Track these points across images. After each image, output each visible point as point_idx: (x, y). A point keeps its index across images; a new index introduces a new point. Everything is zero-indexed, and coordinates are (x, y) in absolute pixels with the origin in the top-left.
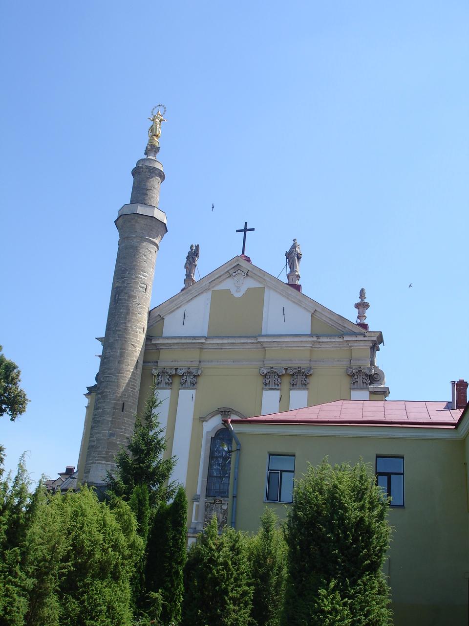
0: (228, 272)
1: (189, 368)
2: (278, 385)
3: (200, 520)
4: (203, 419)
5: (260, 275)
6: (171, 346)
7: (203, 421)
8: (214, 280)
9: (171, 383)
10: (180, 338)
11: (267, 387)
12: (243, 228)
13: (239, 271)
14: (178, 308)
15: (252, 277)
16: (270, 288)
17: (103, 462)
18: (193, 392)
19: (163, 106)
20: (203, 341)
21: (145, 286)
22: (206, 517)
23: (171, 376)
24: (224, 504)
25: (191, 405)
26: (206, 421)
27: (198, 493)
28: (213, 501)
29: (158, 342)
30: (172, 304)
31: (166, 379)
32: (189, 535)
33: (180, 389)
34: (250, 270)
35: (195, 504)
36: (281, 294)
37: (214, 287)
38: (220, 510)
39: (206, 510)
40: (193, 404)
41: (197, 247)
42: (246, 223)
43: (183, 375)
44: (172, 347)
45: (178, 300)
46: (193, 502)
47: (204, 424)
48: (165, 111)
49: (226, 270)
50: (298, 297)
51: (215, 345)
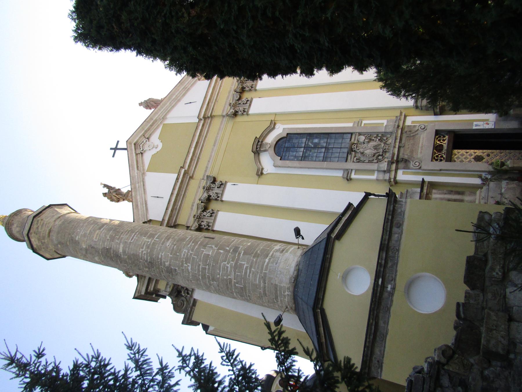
0: (137, 154)
1: (204, 188)
2: (248, 101)
3: (375, 166)
4: (260, 173)
5: (151, 123)
6: (176, 209)
7: (262, 173)
8: (138, 167)
9: (212, 210)
10: (172, 194)
11: (246, 110)
12: (113, 151)
13: (141, 145)
14: (146, 204)
15: (151, 135)
16: (164, 118)
17: (267, 260)
18: (229, 185)
20: (183, 171)
22: (370, 162)
23: (205, 209)
24: (358, 141)
25: (241, 186)
26: (262, 169)
27: (340, 174)
28: (354, 153)
29: (166, 222)
30: (139, 208)
31: (207, 214)
32: (392, 177)
33: (222, 201)
34: (143, 132)
35: (353, 176)
36: (173, 107)
37: (144, 170)
38: (365, 145)
39: (364, 162)
40: (240, 185)
41: (105, 186)
42: (111, 149)
43: (210, 196)
44: (178, 208)
45: (139, 200)
46: (351, 179)
47: (264, 173)
49: (134, 154)
50: (180, 90)
51: (192, 163)
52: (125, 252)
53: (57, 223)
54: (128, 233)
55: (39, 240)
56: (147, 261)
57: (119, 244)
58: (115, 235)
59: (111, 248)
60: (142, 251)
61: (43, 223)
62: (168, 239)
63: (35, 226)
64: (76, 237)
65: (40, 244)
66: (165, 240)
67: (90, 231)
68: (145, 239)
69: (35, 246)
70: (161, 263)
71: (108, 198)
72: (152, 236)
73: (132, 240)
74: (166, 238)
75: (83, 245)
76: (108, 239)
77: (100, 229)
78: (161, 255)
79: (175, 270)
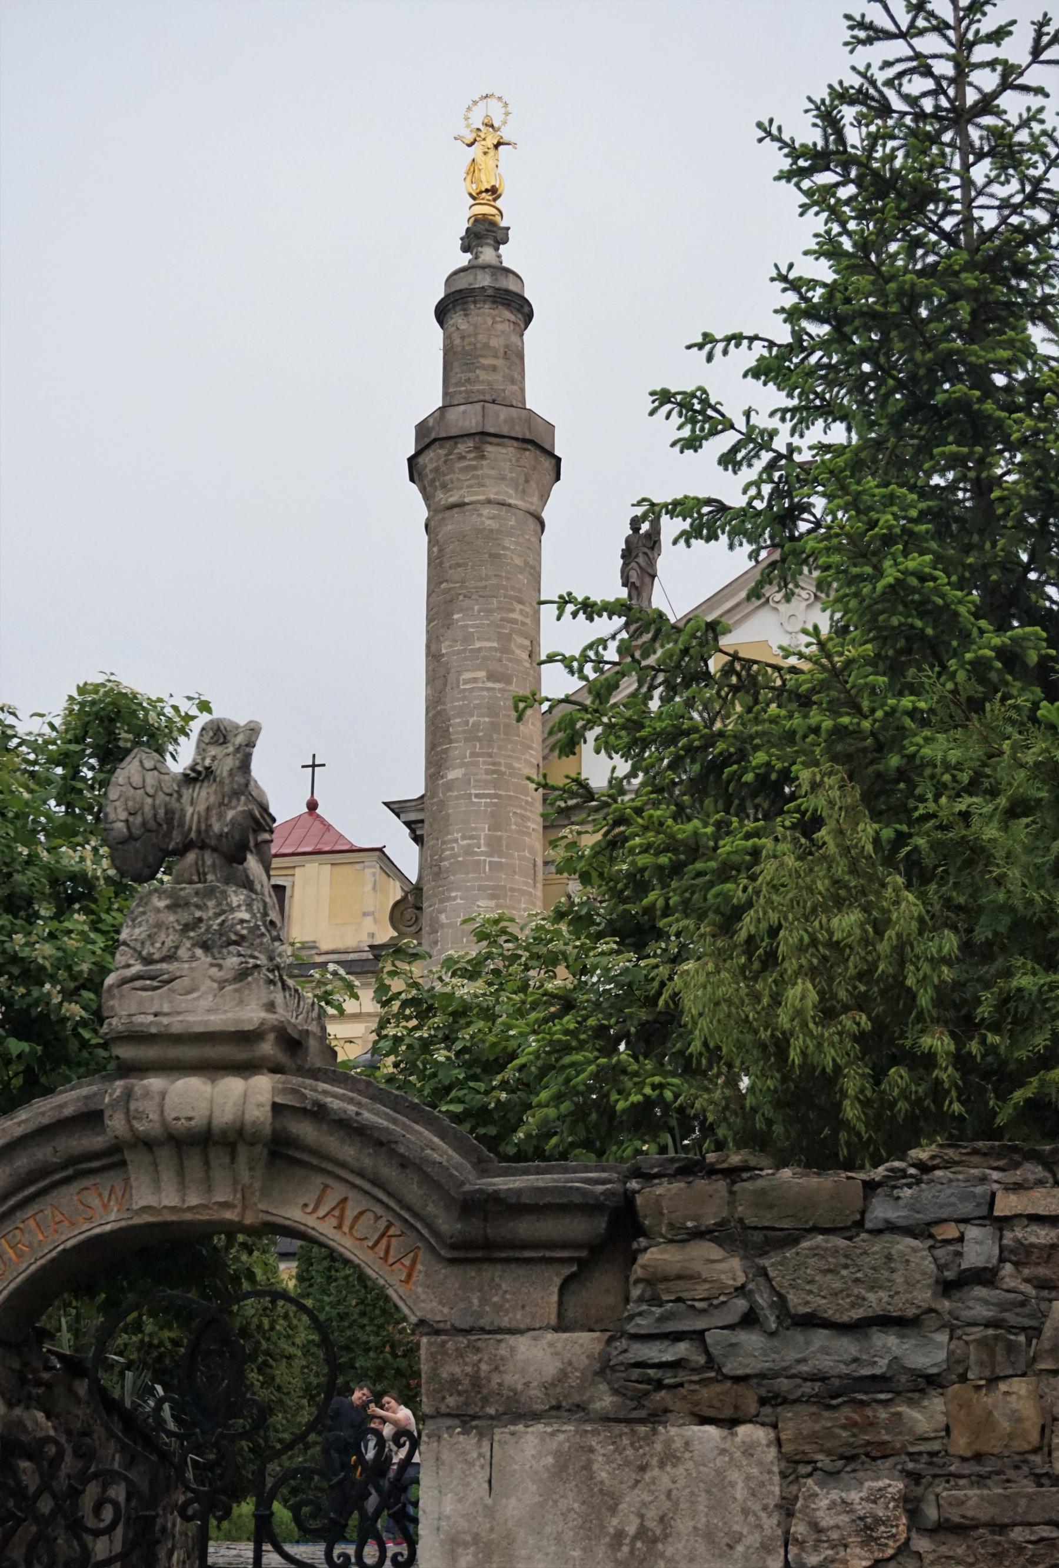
19: (500, 98)
21: (527, 643)
48: (507, 114)
52: (449, 790)
53: (486, 511)
54: (494, 772)
55: (436, 470)
56: (442, 860)
57: (462, 765)
58: (479, 739)
59: (451, 741)
60: (456, 841)
61: (475, 468)
62: (493, 897)
63: (461, 448)
64: (460, 611)
65: (430, 476)
66: (488, 888)
67: (480, 649)
68: (485, 831)
69: (421, 460)
70: (442, 901)
71: (628, 541)
72: (494, 845)
73: (477, 796)
74: (494, 888)
75: (447, 643)
76: (467, 722)
77: (491, 677)
78: (455, 898)
79: (436, 943)
